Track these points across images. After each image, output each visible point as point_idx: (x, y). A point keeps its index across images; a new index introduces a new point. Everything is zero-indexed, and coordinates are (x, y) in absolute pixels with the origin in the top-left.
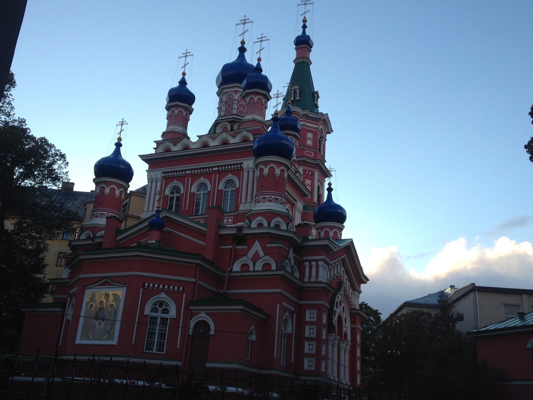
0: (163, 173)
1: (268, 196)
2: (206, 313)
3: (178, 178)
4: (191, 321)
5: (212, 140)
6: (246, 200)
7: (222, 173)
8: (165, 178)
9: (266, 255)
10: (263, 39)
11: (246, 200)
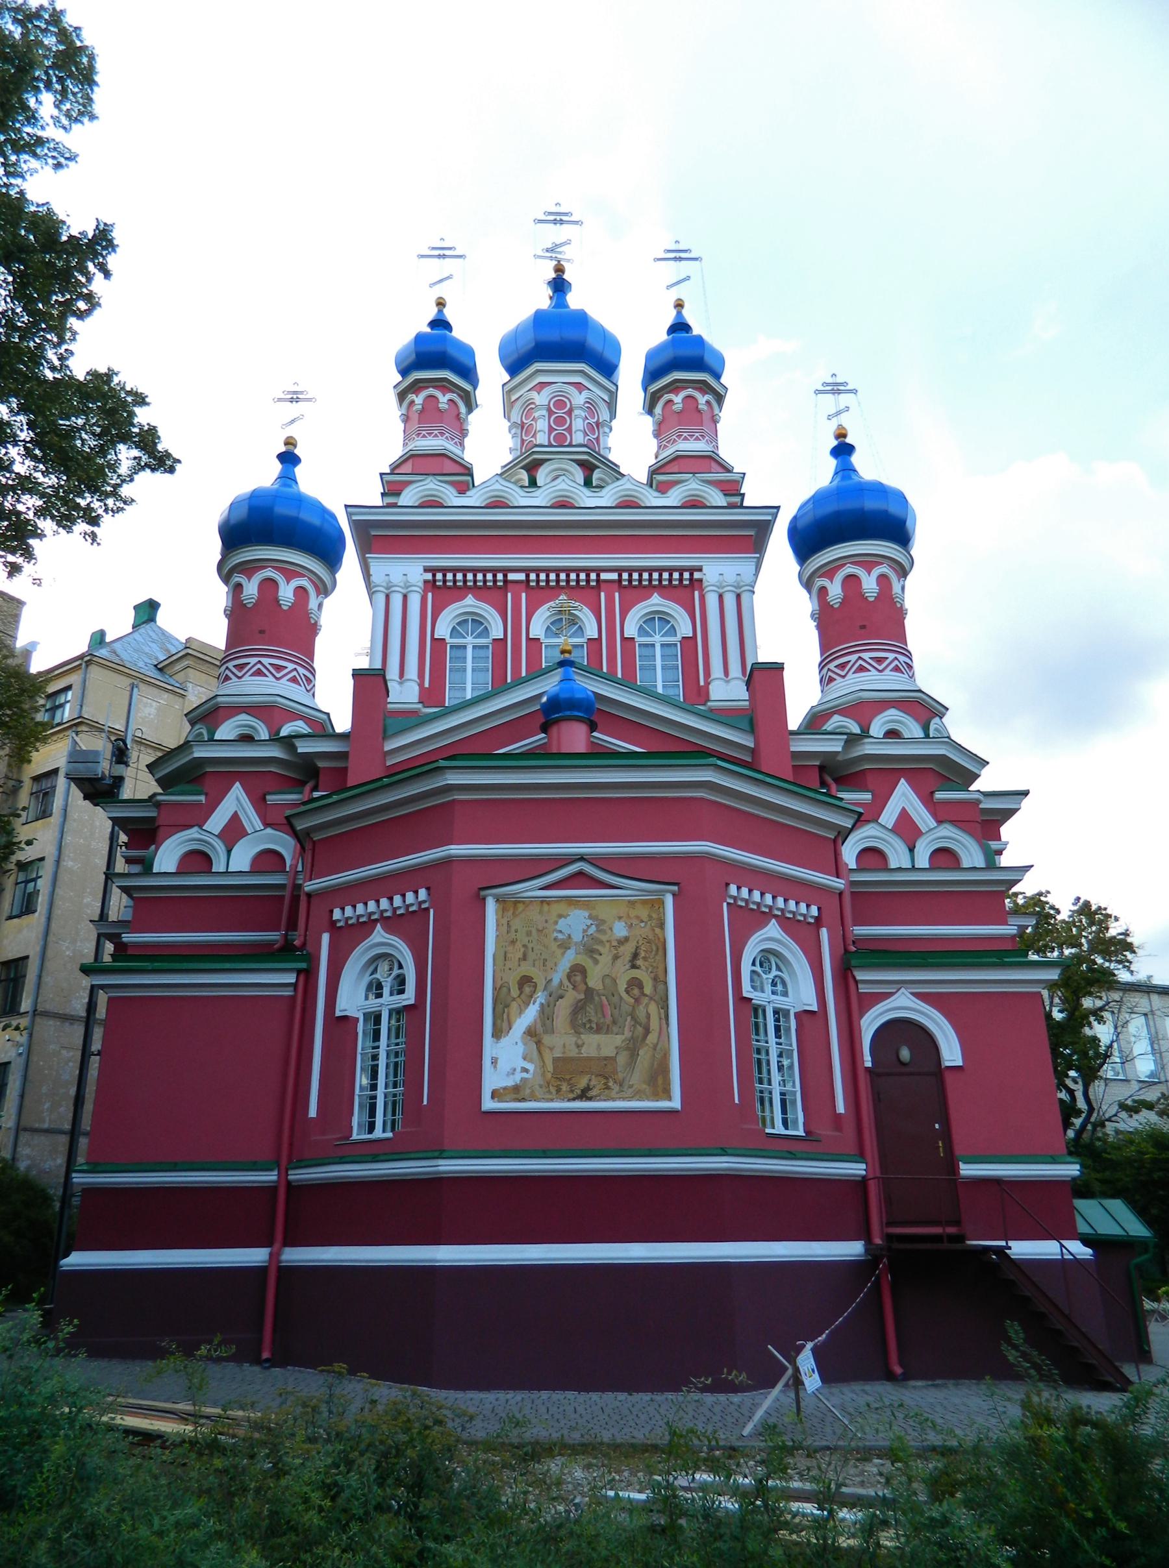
0: (426, 570)
2: (918, 996)
3: (480, 591)
4: (862, 1021)
6: (726, 673)
7: (633, 588)
8: (430, 585)
9: (940, 822)
11: (726, 673)
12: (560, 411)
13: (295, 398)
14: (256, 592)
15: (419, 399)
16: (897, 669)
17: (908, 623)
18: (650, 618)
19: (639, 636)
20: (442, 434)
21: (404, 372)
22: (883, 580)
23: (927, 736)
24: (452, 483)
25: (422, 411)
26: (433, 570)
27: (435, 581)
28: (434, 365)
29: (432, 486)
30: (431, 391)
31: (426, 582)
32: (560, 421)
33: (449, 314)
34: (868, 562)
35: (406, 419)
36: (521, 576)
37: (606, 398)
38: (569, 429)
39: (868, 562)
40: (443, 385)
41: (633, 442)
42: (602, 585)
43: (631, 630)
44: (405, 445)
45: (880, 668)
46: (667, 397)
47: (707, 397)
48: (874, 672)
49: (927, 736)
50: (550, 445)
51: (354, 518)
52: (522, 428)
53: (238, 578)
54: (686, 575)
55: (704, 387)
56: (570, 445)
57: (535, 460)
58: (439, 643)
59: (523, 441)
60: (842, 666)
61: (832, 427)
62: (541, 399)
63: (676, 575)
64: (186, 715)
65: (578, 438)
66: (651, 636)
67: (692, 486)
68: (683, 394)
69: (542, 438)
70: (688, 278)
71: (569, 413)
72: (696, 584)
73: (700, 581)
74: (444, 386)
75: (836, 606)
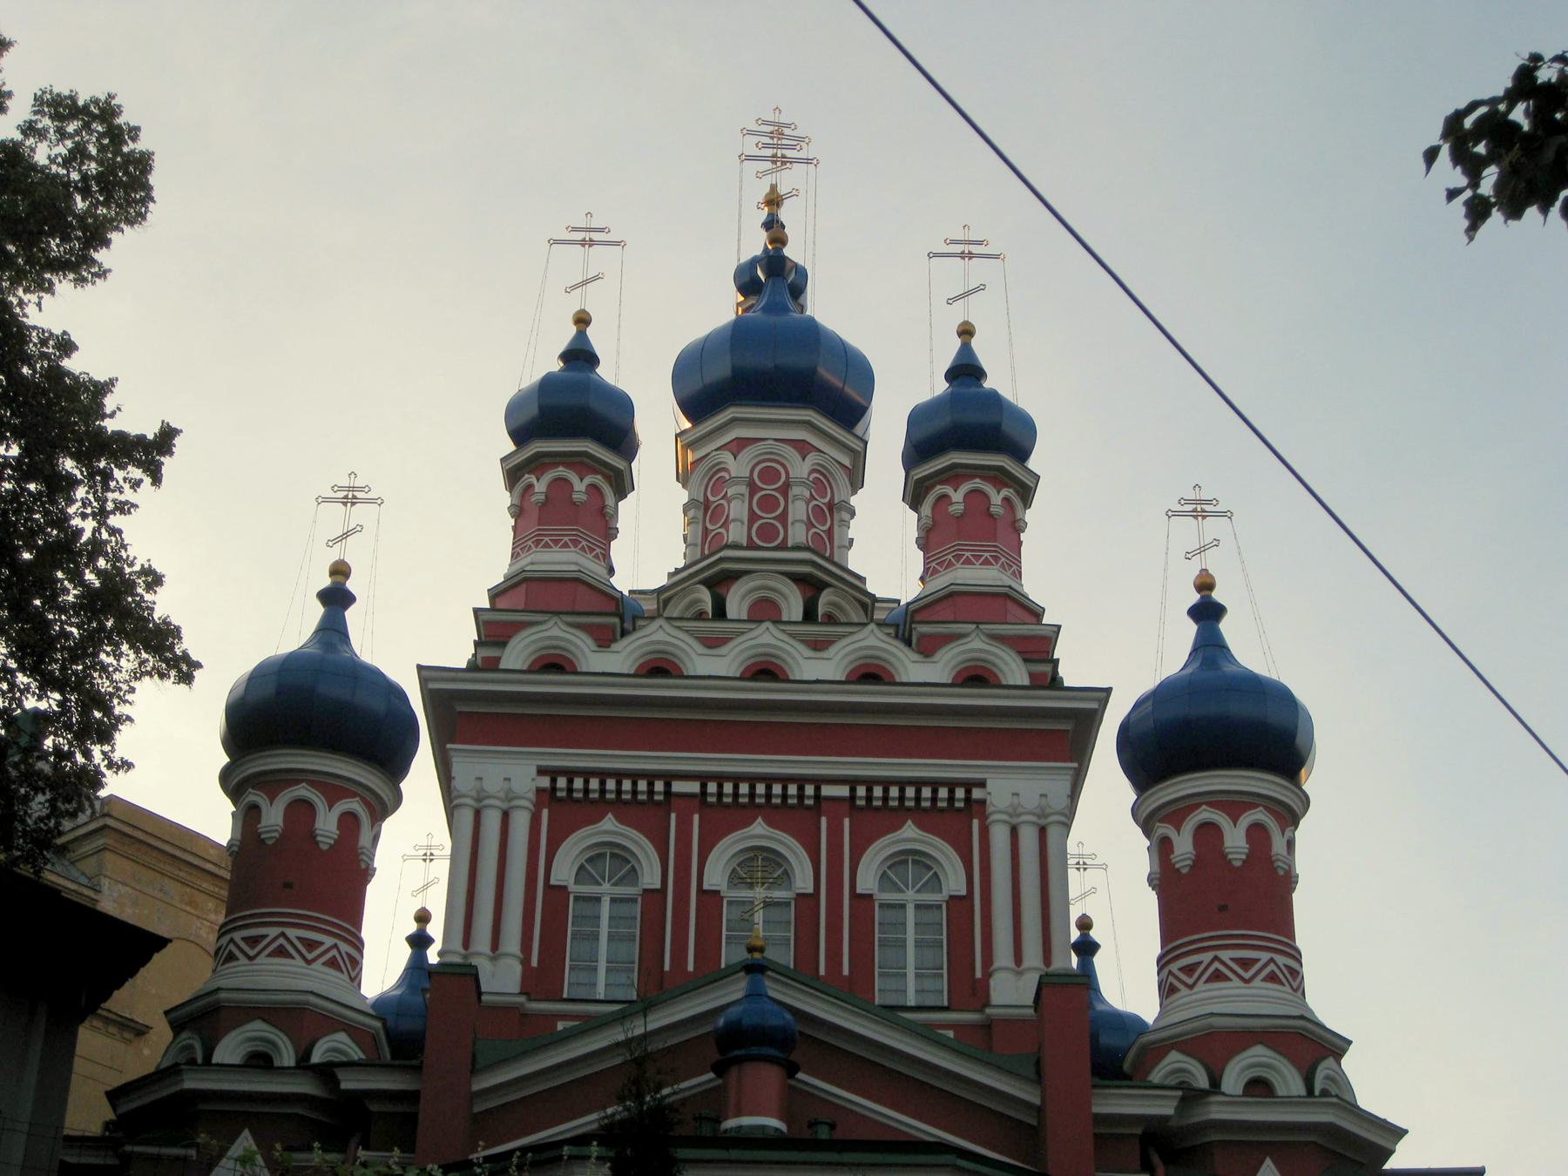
0: (541, 771)
1: (1206, 957)
3: (626, 809)
5: (701, 649)
7: (873, 813)
8: (546, 797)
10: (596, 236)
12: (769, 488)
13: (350, 498)
14: (280, 821)
15: (541, 486)
16: (1272, 978)
17: (1301, 900)
18: (900, 860)
19: (882, 889)
20: (575, 543)
21: (520, 435)
22: (1257, 834)
23: (1310, 1092)
24: (588, 629)
25: (544, 505)
27: (554, 789)
28: (568, 427)
29: (556, 632)
30: (561, 471)
31: (539, 791)
32: (768, 503)
33: (597, 338)
34: (1234, 805)
35: (518, 512)
36: (693, 787)
37: (847, 462)
38: (783, 518)
39: (1234, 805)
40: (582, 463)
41: (885, 550)
42: (824, 805)
43: (867, 881)
44: (515, 556)
45: (1247, 976)
46: (940, 489)
47: (1005, 492)
48: (1236, 982)
49: (1310, 1092)
50: (751, 546)
51: (432, 686)
52: (704, 513)
53: (253, 796)
54: (960, 793)
55: (1000, 478)
56: (782, 547)
57: (723, 571)
58: (557, 894)
59: (706, 531)
60: (1189, 970)
61: (1192, 571)
62: (738, 466)
63: (943, 793)
64: (166, 1013)
65: (797, 534)
66: (901, 891)
67: (975, 645)
68: (966, 487)
69: (737, 533)
70: (981, 288)
71: (785, 490)
72: (975, 808)
73: (983, 802)
74: (582, 463)
75: (1184, 871)
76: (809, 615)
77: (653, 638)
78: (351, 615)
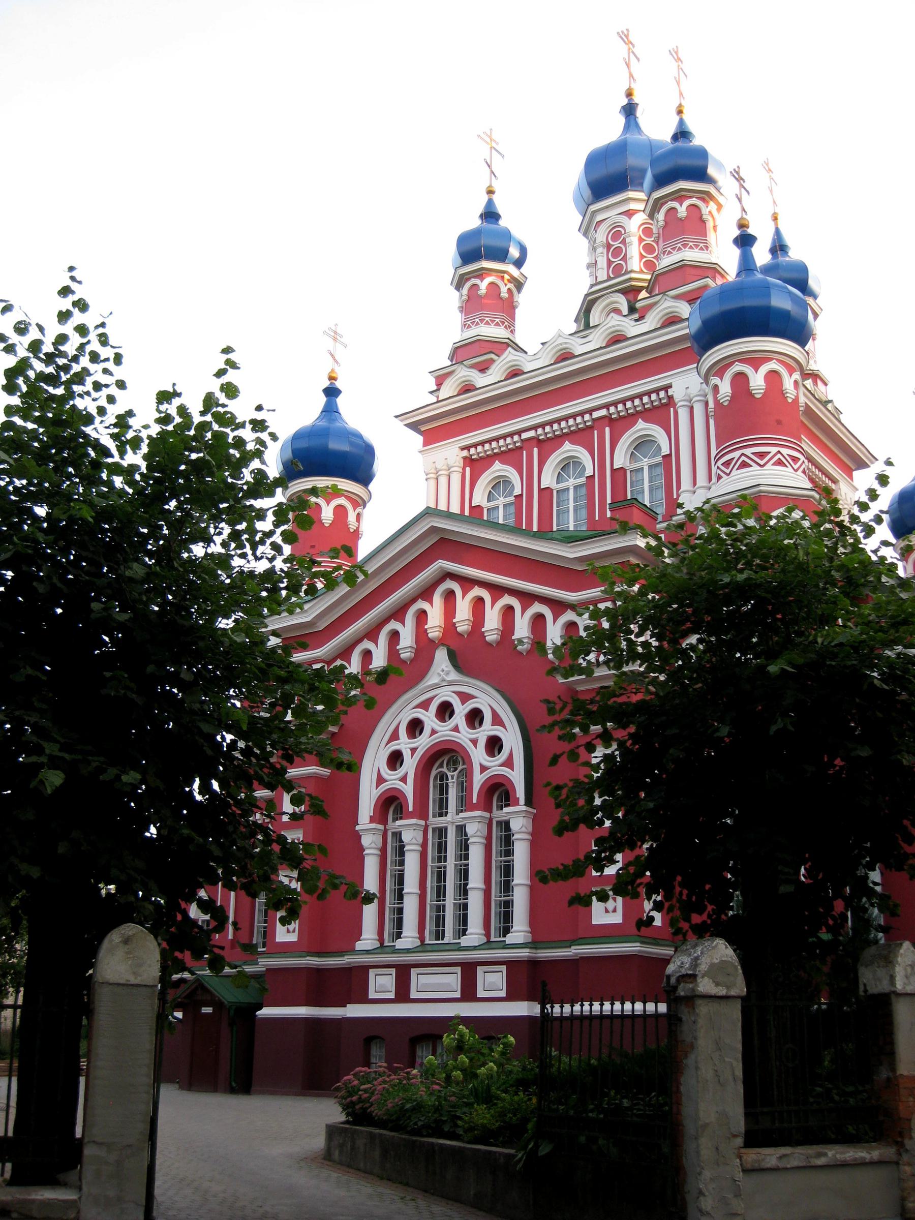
0: (463, 449)
8: (469, 461)
26: (468, 448)
31: (465, 458)
76: (632, 310)
77: (507, 360)
78: (340, 400)
